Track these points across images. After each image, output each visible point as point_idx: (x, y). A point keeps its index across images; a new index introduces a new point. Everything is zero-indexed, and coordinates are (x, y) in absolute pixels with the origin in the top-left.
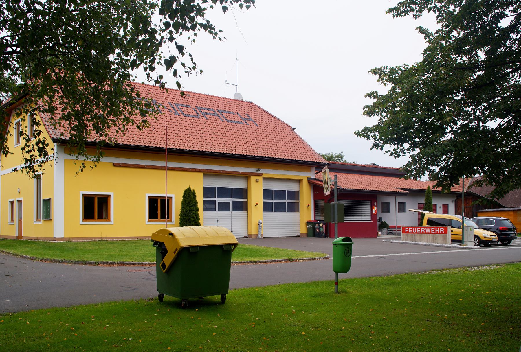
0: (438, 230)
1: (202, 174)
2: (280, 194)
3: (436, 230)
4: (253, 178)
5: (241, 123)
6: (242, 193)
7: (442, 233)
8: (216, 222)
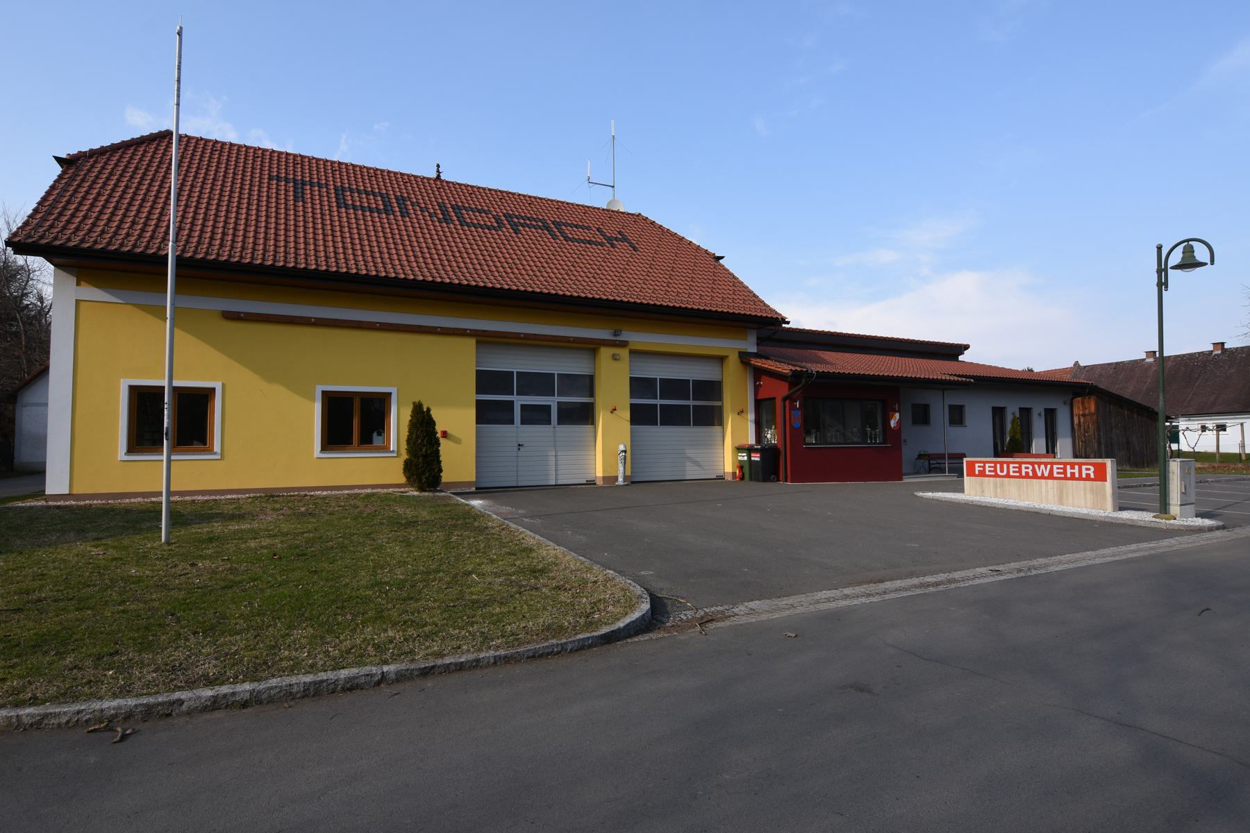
0: (1076, 471)
1: (472, 342)
2: (673, 387)
3: (1069, 471)
4: (605, 353)
5: (602, 244)
6: (588, 384)
7: (1088, 478)
8: (516, 449)
